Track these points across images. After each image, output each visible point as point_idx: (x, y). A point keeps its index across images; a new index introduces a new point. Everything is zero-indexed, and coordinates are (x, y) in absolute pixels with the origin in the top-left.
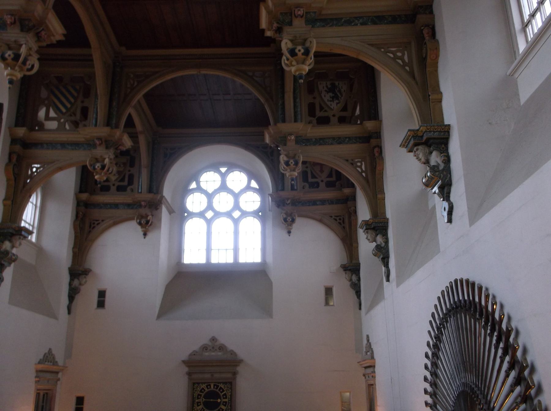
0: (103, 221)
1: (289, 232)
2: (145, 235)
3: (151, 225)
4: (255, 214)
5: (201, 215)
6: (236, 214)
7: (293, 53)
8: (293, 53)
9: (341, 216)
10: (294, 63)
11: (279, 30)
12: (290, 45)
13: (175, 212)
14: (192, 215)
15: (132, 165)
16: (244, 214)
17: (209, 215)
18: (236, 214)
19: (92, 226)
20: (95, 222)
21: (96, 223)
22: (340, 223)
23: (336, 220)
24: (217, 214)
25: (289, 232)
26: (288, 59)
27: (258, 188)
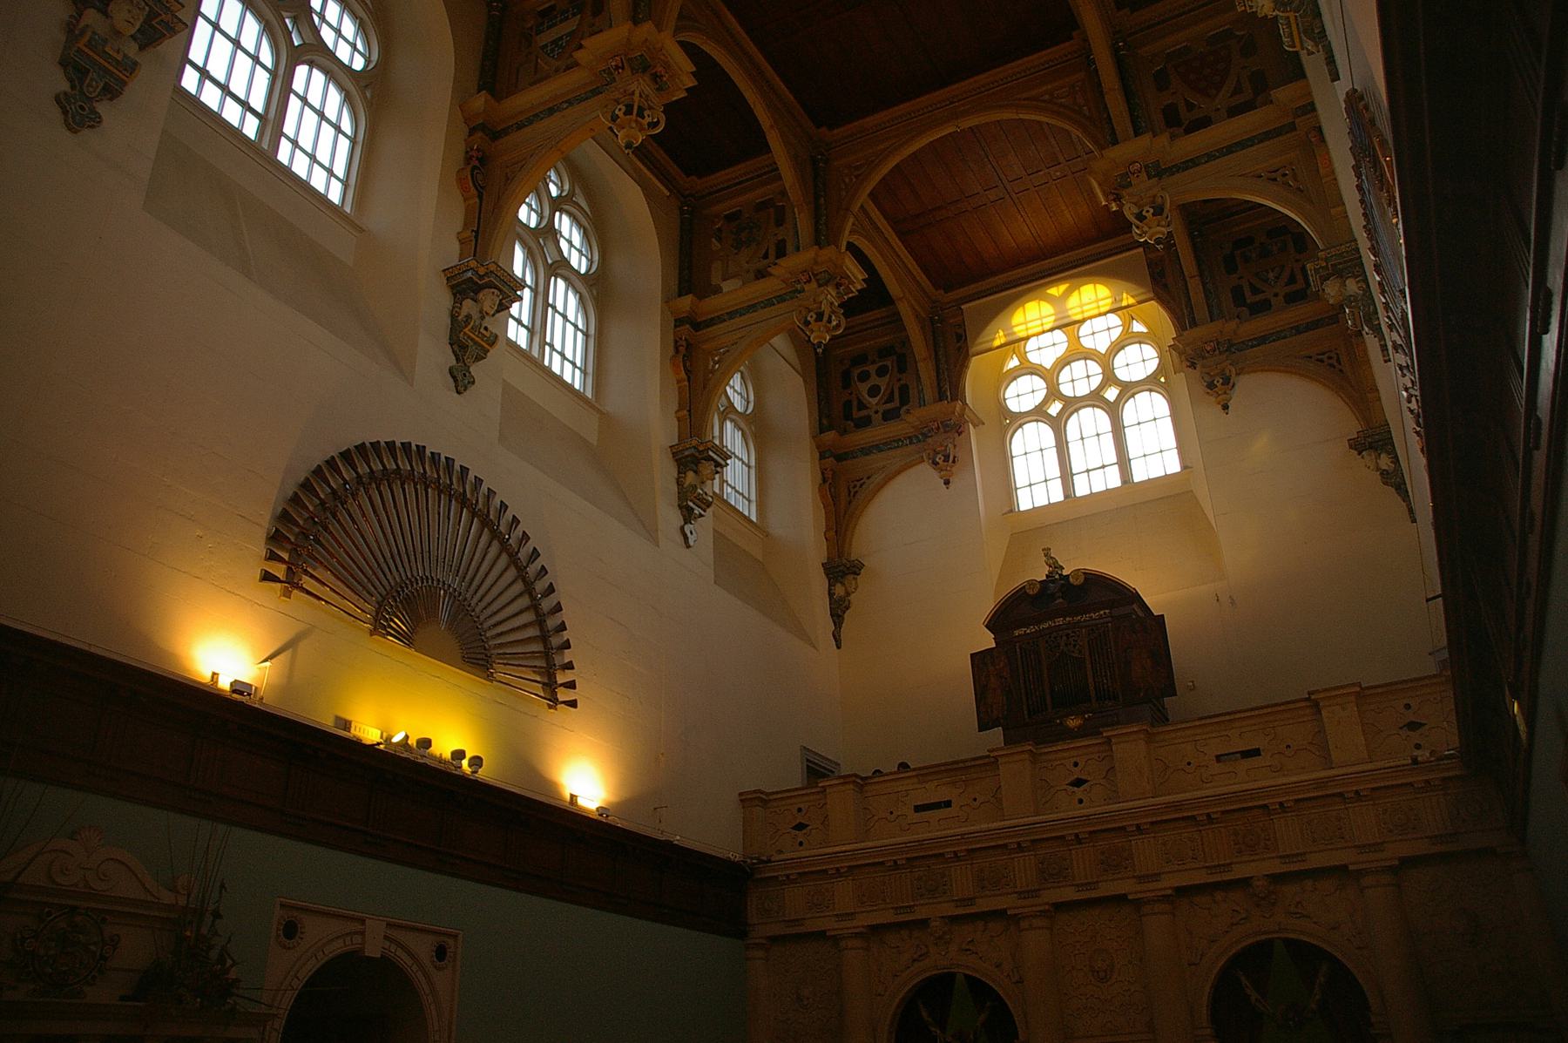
0: (868, 478)
1: (1226, 407)
2: (947, 483)
3: (954, 462)
4: (1150, 383)
5: (1039, 413)
6: (1111, 394)
7: (1140, 217)
8: (1140, 217)
9: (1331, 351)
10: (1146, 229)
11: (1118, 199)
12: (1136, 211)
13: (983, 424)
14: (1019, 419)
15: (902, 370)
16: (1129, 390)
17: (1055, 408)
18: (1111, 394)
19: (853, 491)
20: (856, 483)
21: (858, 484)
22: (1332, 366)
23: (1322, 361)
24: (1073, 405)
25: (1226, 407)
26: (1138, 227)
27: (1145, 330)
